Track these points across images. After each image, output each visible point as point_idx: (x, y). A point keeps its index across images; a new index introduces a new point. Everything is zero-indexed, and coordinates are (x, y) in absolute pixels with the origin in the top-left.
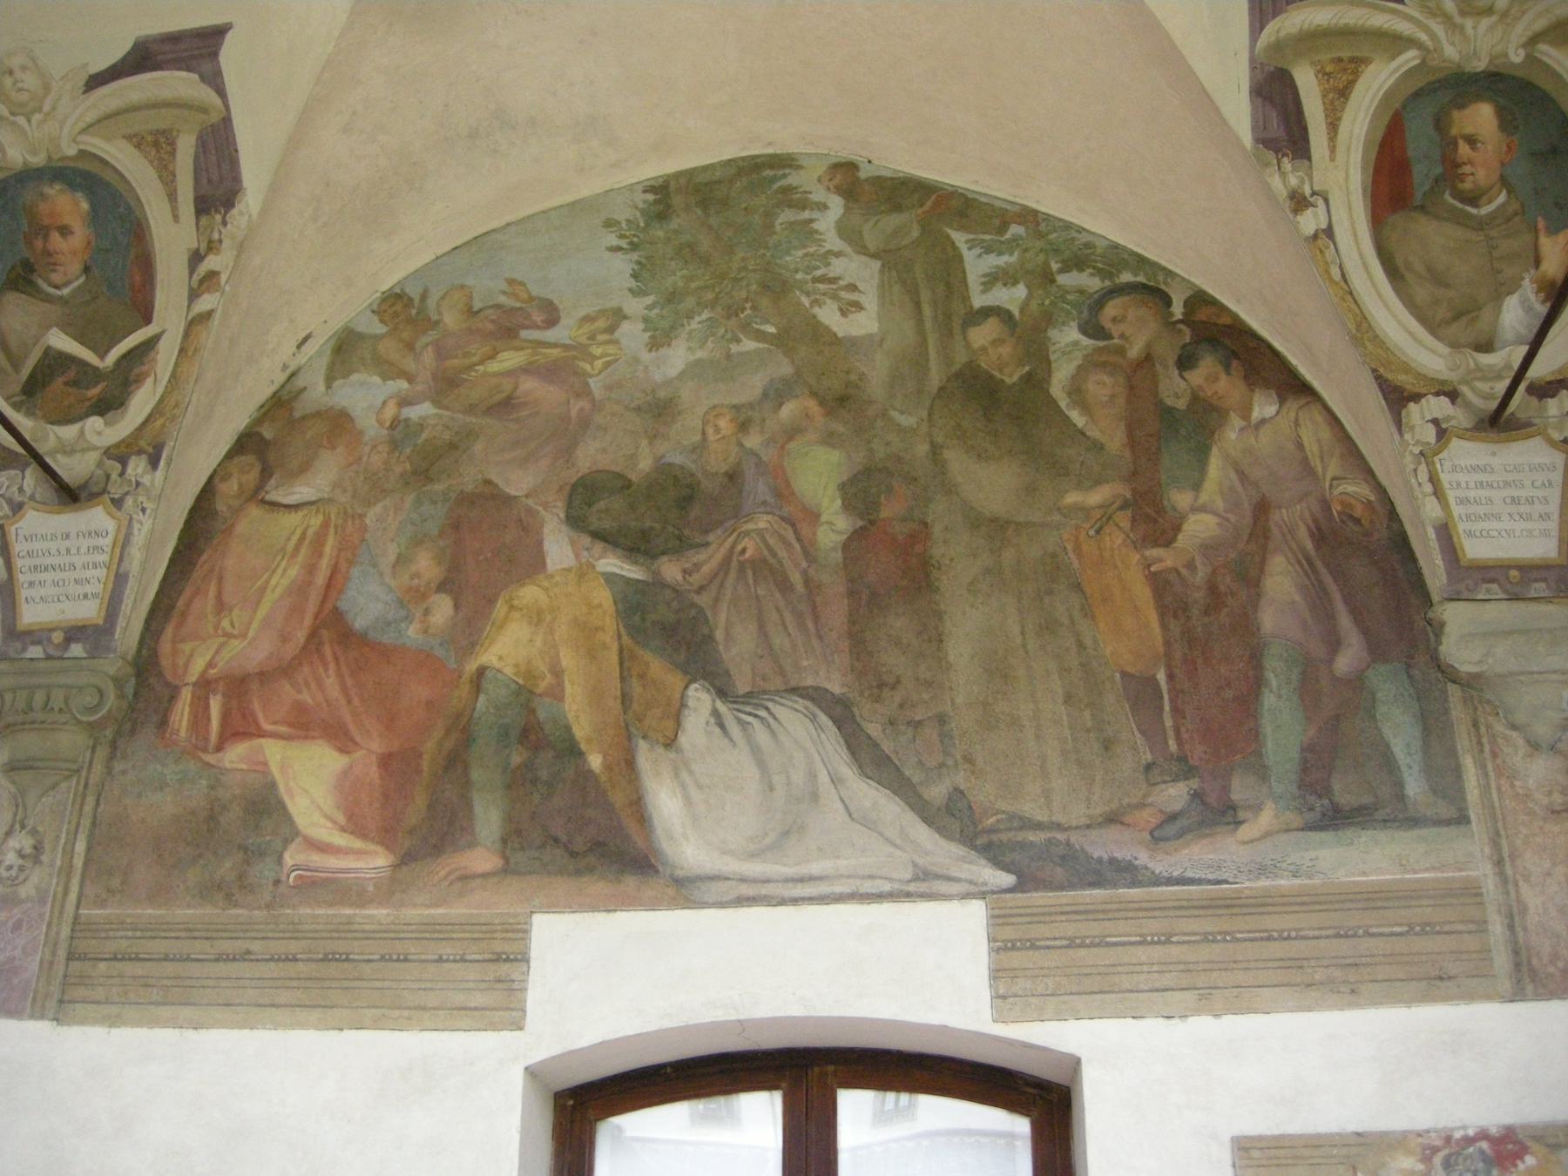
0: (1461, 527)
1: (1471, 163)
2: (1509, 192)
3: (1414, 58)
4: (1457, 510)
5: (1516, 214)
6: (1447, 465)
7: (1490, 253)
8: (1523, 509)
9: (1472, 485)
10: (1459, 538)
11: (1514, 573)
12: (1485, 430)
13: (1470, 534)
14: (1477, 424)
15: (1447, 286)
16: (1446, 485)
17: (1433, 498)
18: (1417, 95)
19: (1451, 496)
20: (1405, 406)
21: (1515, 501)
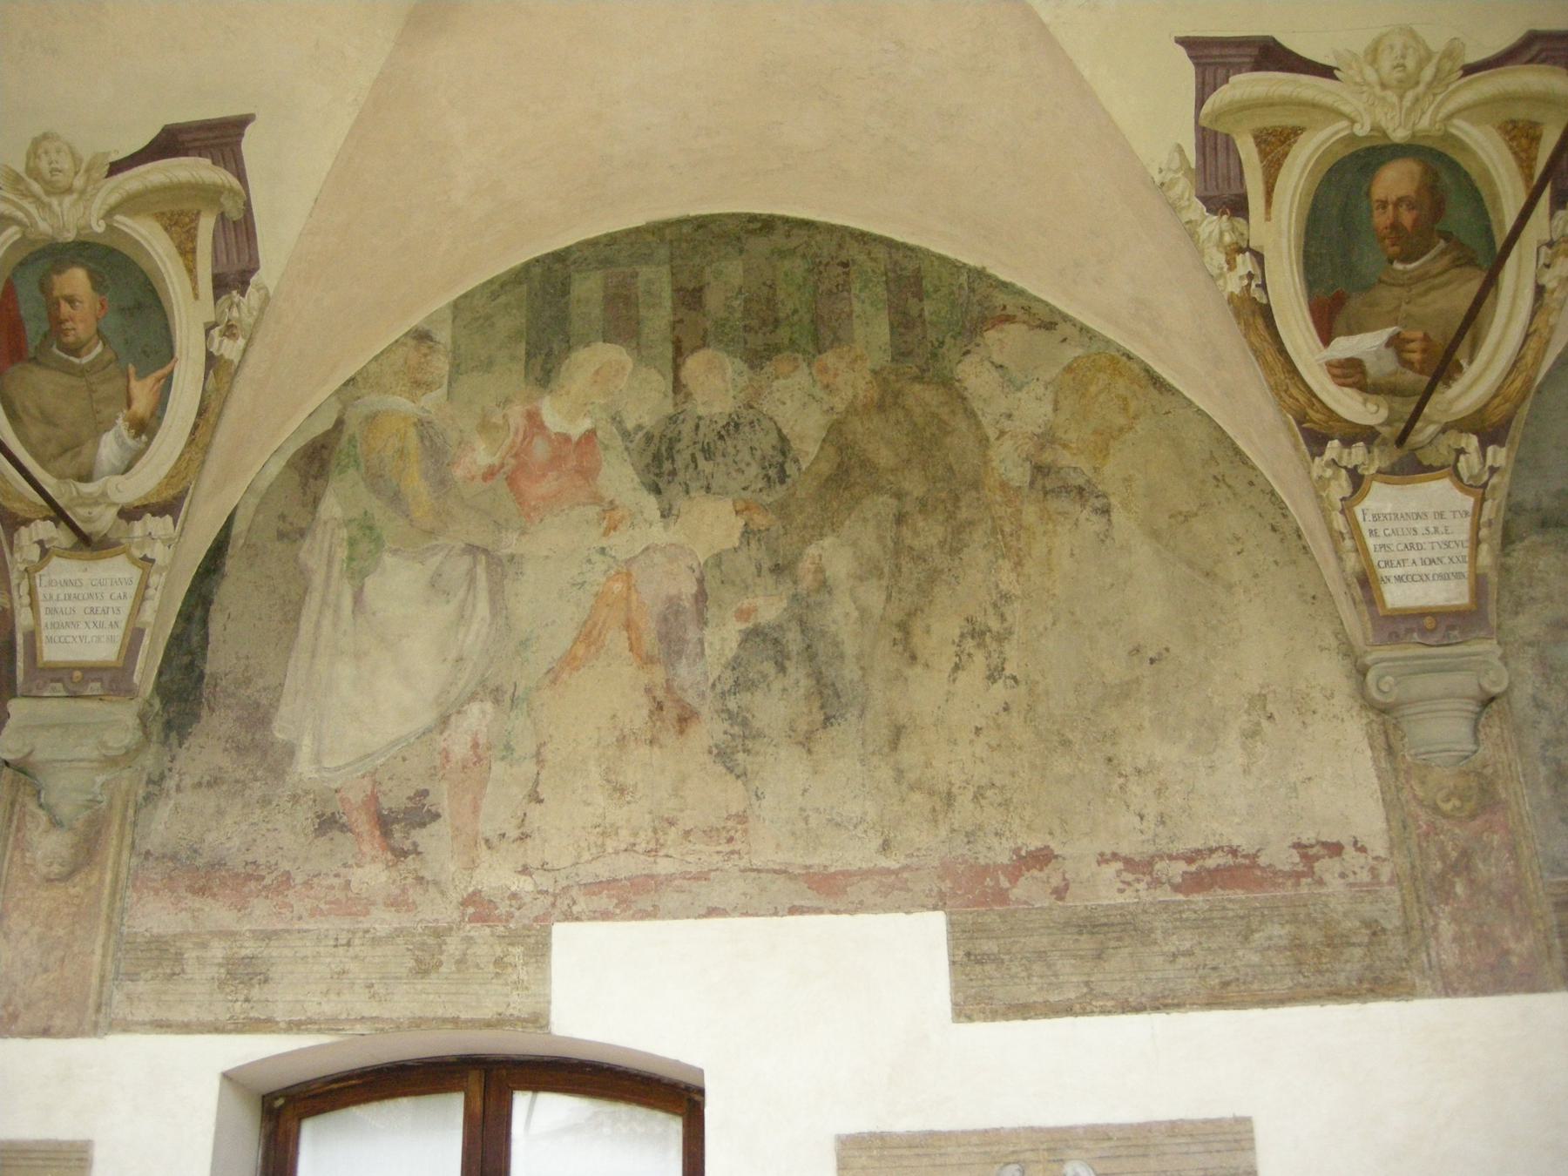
0: (45, 633)
1: (72, 319)
2: (104, 345)
3: (15, 233)
4: (45, 618)
5: (110, 362)
6: (45, 580)
7: (91, 396)
8: (98, 618)
9: (62, 597)
10: (41, 642)
11: (78, 674)
12: (81, 550)
13: (51, 640)
14: (75, 544)
15: (56, 425)
16: (41, 597)
17: (29, 609)
18: (23, 264)
19: (43, 605)
20: (17, 530)
21: (93, 611)
